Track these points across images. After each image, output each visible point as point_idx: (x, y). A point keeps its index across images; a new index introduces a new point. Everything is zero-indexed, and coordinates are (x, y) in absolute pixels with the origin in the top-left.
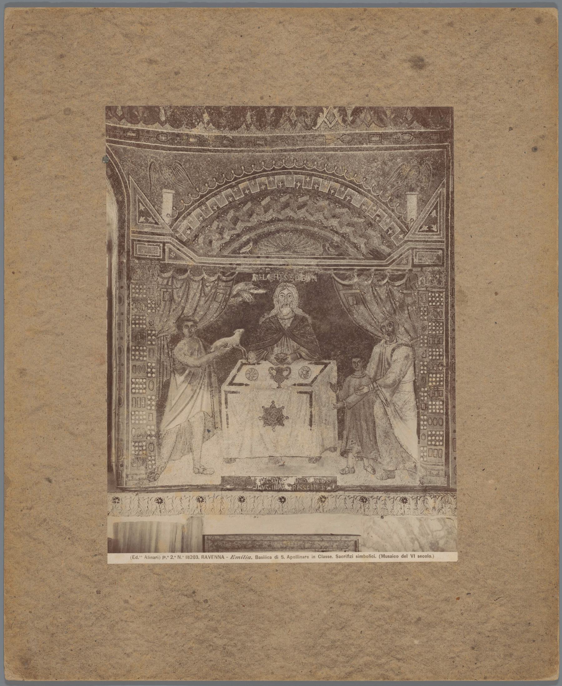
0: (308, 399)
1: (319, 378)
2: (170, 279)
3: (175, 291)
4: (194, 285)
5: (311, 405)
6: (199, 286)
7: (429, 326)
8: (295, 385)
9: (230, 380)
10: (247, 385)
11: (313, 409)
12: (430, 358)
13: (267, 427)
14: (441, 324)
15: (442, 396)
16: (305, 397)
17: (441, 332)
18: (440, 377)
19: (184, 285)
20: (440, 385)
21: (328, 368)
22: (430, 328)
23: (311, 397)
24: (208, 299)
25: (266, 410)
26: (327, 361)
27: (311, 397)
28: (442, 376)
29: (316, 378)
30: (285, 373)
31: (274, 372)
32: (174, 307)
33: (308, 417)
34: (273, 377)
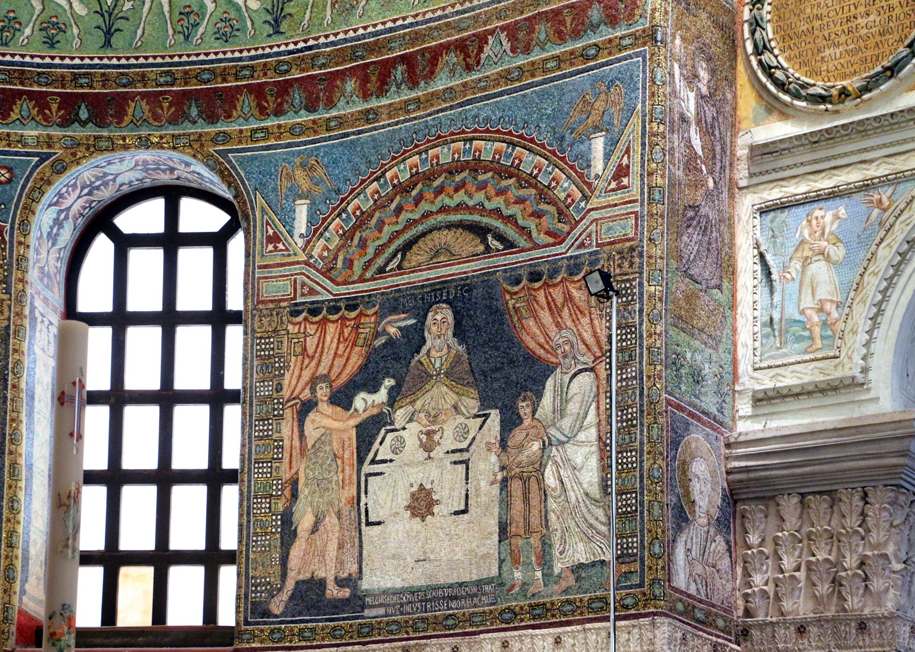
1: (477, 438)
5: (467, 479)
8: (448, 452)
10: (391, 461)
11: (469, 485)
23: (467, 469)
27: (467, 469)
29: (474, 438)
30: (436, 437)
32: (307, 361)
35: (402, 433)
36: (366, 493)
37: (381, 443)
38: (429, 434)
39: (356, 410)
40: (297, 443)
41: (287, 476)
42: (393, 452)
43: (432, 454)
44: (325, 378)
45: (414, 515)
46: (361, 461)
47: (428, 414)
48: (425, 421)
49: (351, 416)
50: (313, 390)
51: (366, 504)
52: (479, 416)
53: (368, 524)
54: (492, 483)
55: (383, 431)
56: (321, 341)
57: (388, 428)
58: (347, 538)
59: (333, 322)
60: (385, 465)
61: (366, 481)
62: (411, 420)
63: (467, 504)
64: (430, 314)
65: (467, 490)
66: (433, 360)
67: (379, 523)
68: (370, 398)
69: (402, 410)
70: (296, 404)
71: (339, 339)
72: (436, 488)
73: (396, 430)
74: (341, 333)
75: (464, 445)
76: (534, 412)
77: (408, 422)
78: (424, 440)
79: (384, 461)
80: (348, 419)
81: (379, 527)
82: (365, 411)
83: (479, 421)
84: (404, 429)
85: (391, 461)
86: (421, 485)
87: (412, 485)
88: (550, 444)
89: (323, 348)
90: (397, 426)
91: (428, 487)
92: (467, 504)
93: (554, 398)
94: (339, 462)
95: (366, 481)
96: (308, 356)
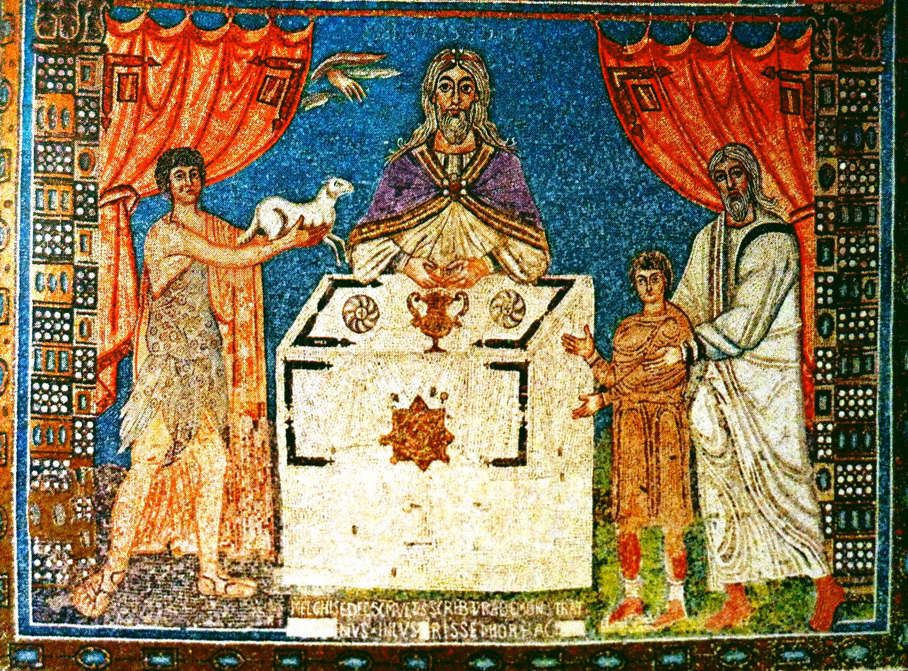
0: (517, 385)
1: (546, 325)
2: (139, 38)
3: (150, 71)
4: (203, 56)
5: (523, 400)
6: (215, 56)
7: (841, 172)
8: (479, 344)
9: (301, 327)
10: (345, 343)
11: (528, 414)
12: (843, 263)
13: (402, 464)
14: (873, 166)
15: (872, 372)
16: (511, 379)
17: (872, 189)
18: (866, 320)
19: (177, 54)
20: (867, 341)
21: (572, 292)
22: (842, 178)
24: (241, 96)
25: (399, 416)
26: (569, 277)
28: (872, 314)
29: (536, 326)
30: (452, 310)
31: (423, 309)
33: (515, 433)
34: (417, 320)
35: (369, 291)
36: (288, 400)
37: (322, 304)
38: (436, 302)
39: (260, 231)
41: (104, 345)
42: (349, 326)
43: (442, 344)
44: (188, 156)
45: (400, 456)
46: (273, 336)
47: (430, 266)
48: (423, 276)
49: (250, 242)
50: (163, 178)
51: (289, 422)
52: (550, 283)
53: (295, 460)
54: (579, 414)
55: (325, 283)
56: (181, 77)
57: (338, 276)
58: (245, 482)
59: (207, 44)
60: (331, 349)
61: (288, 377)
62: (390, 269)
63: (522, 446)
64: (436, 66)
65: (524, 423)
66: (441, 157)
67: (320, 462)
68: (293, 211)
69: (367, 246)
70: (125, 200)
71: (219, 82)
72: (450, 406)
73: (356, 284)
74: (225, 69)
75: (515, 335)
76: (668, 292)
77: (383, 272)
78: (423, 313)
79: (331, 342)
80: (242, 246)
81: (323, 470)
82: (283, 233)
83: (549, 293)
84: (375, 284)
85: (345, 343)
86: (418, 399)
87: (396, 398)
88: (703, 355)
89: (183, 93)
90: (358, 275)
91: (434, 404)
92: (522, 446)
93: (711, 272)
94: (224, 329)
95: (288, 377)
96: (150, 105)
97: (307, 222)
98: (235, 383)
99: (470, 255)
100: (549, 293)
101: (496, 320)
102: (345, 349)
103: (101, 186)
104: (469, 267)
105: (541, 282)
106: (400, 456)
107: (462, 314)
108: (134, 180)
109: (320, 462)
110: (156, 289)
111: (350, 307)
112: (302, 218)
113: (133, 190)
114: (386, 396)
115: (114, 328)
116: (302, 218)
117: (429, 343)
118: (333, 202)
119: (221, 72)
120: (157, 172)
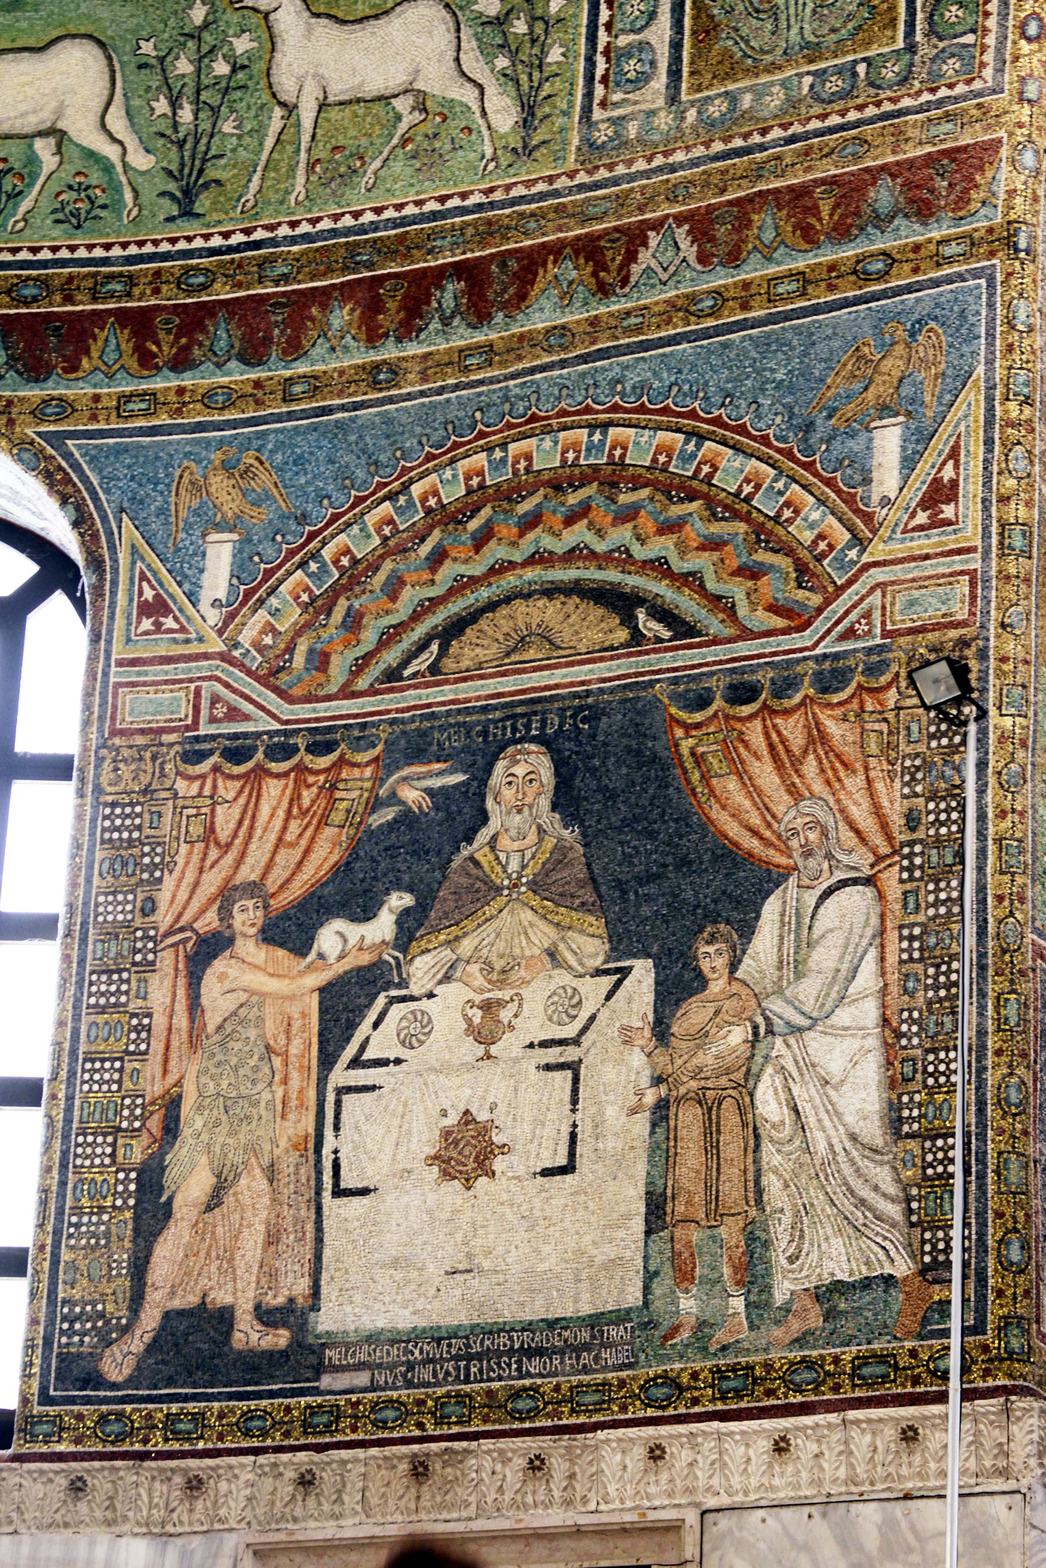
8: (531, 1046)
10: (398, 1061)
29: (592, 1018)
31: (477, 1015)
35: (425, 1004)
36: (337, 1128)
39: (321, 956)
40: (181, 1021)
42: (403, 1043)
46: (327, 1061)
51: (336, 1152)
52: (607, 972)
55: (381, 1001)
59: (278, 776)
62: (447, 978)
67: (364, 1192)
71: (289, 813)
73: (412, 998)
74: (296, 798)
75: (570, 1031)
76: (734, 966)
77: (440, 982)
78: (477, 1020)
83: (608, 981)
84: (431, 995)
85: (398, 1061)
89: (252, 827)
90: (415, 989)
91: (483, 1116)
97: (368, 942)
98: (283, 1117)
99: (528, 953)
100: (608, 981)
101: (550, 1019)
102: (398, 1068)
103: (161, 931)
104: (527, 967)
105: (599, 972)
106: (447, 1175)
107: (516, 1016)
108: (196, 920)
109: (364, 1192)
110: (211, 1028)
111: (404, 1024)
112: (363, 938)
113: (193, 930)
114: (435, 1112)
115: (165, 1072)
116: (363, 938)
117: (480, 1050)
118: (394, 918)
119: (292, 800)
120: (220, 908)
